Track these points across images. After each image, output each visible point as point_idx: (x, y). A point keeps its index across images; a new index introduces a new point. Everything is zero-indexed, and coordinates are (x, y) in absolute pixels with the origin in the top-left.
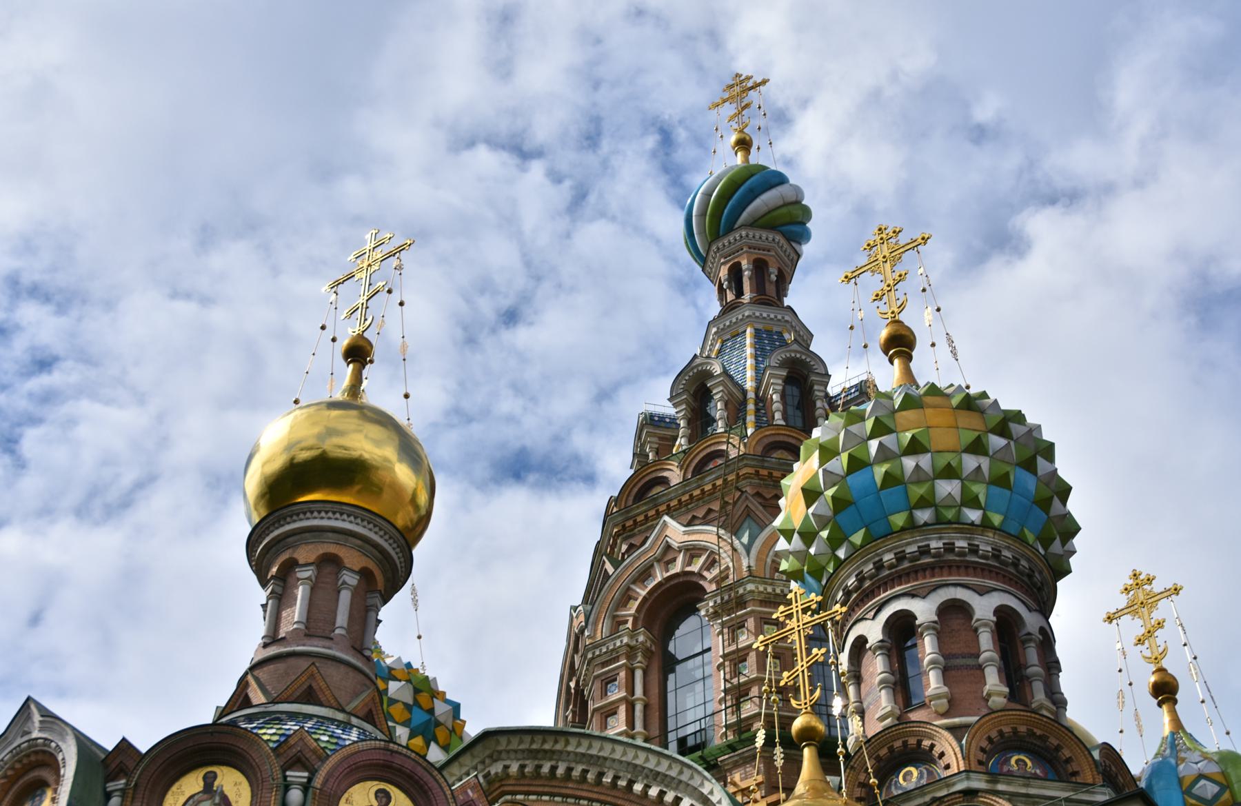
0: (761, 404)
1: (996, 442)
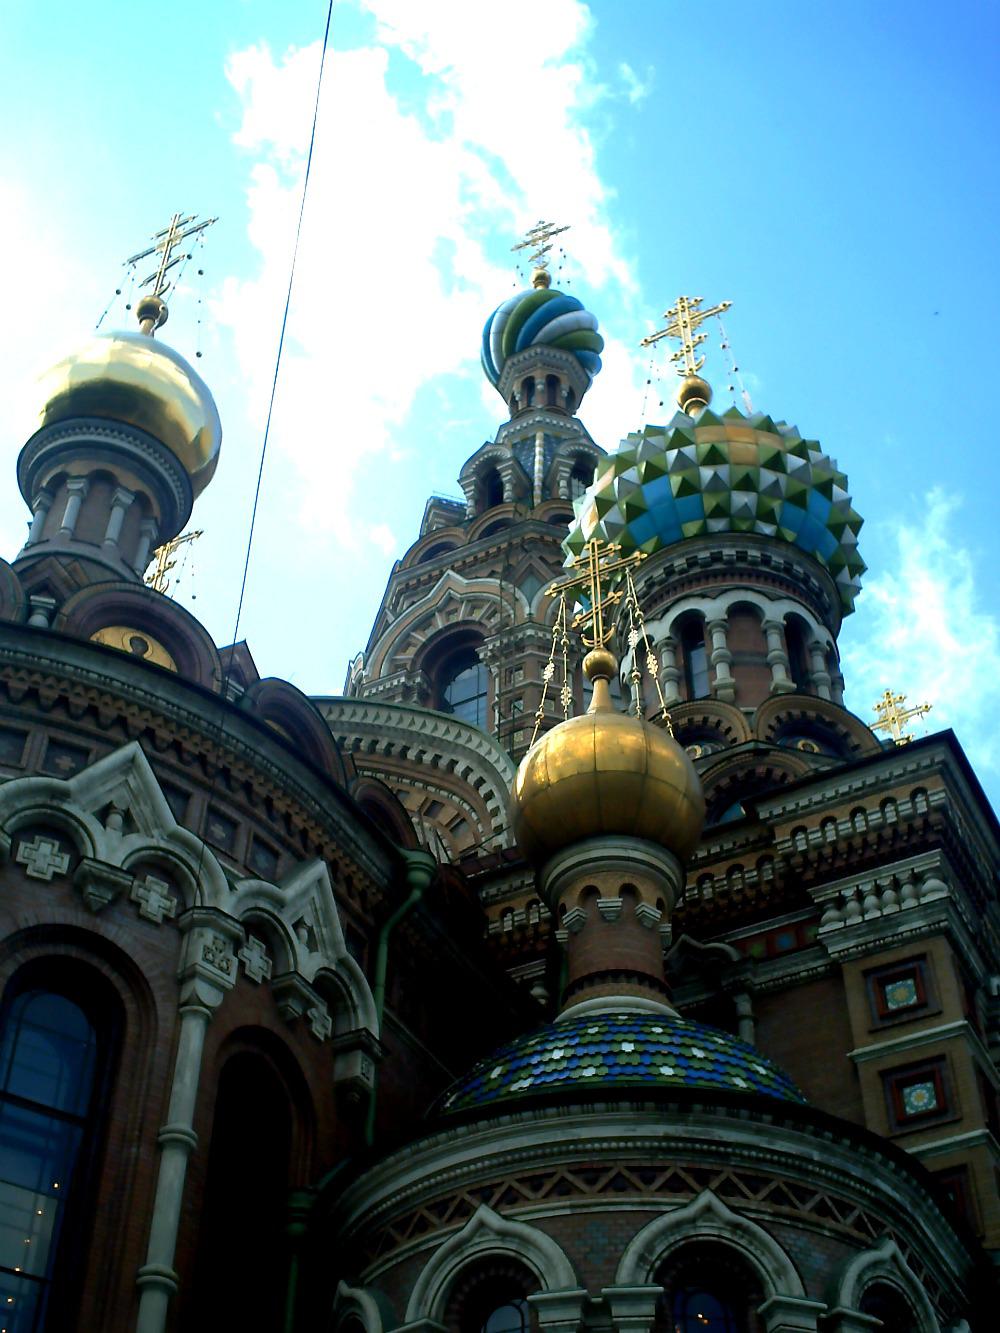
0: (547, 492)
1: (794, 462)
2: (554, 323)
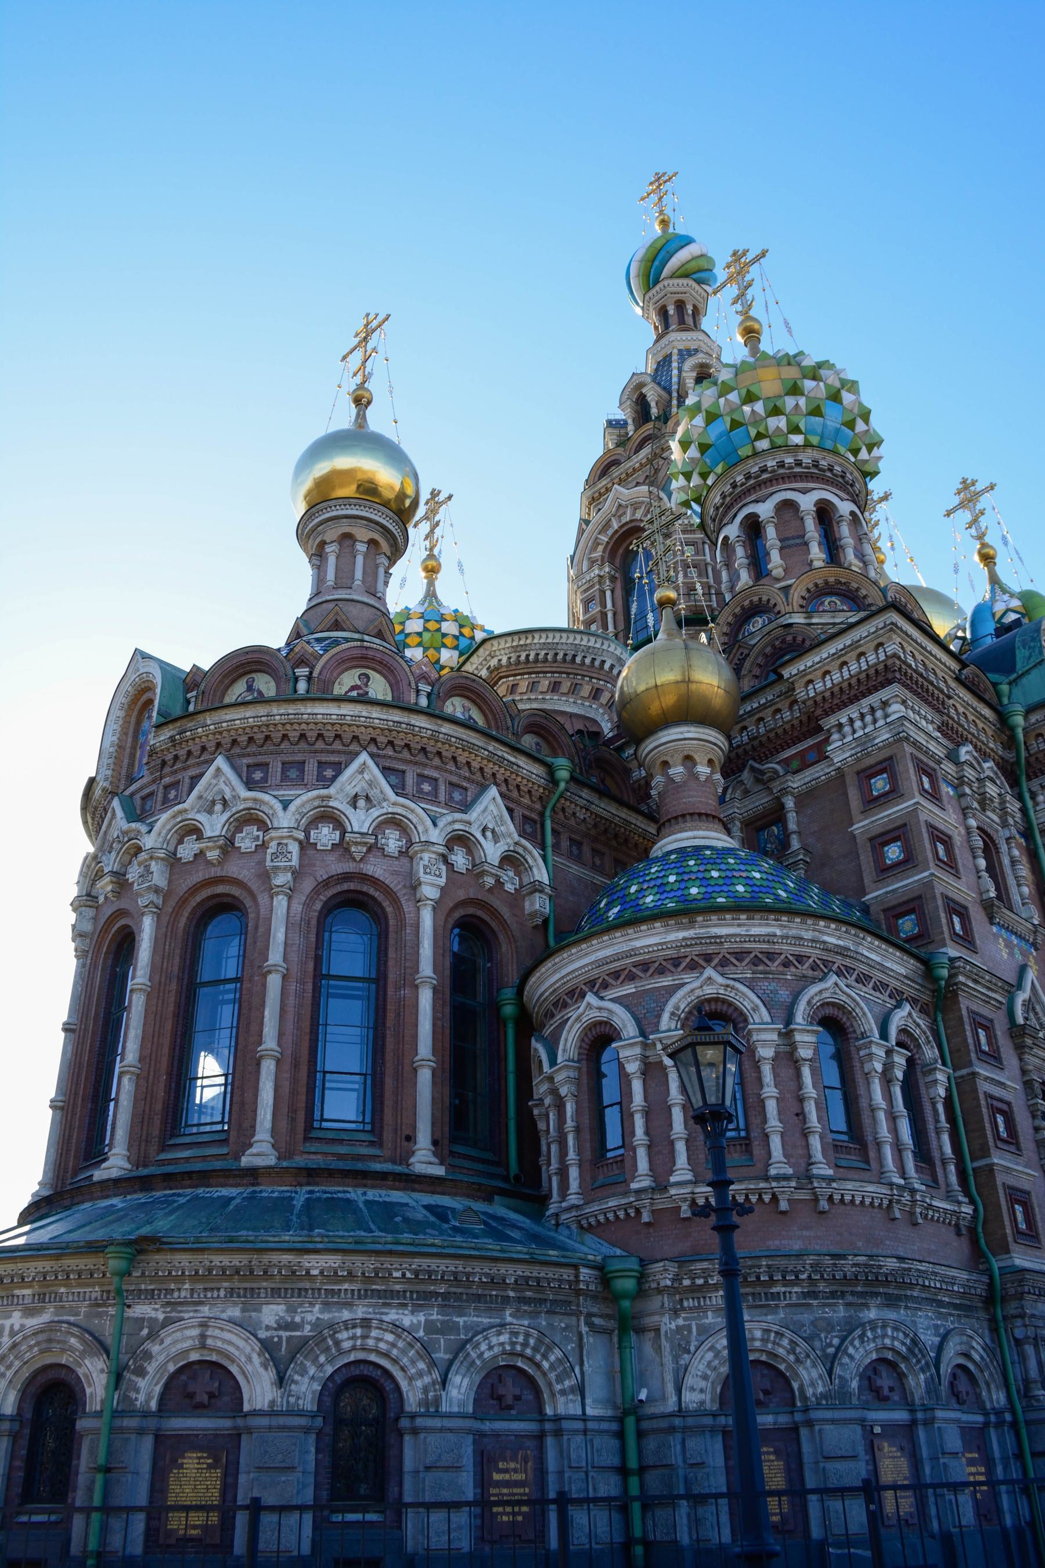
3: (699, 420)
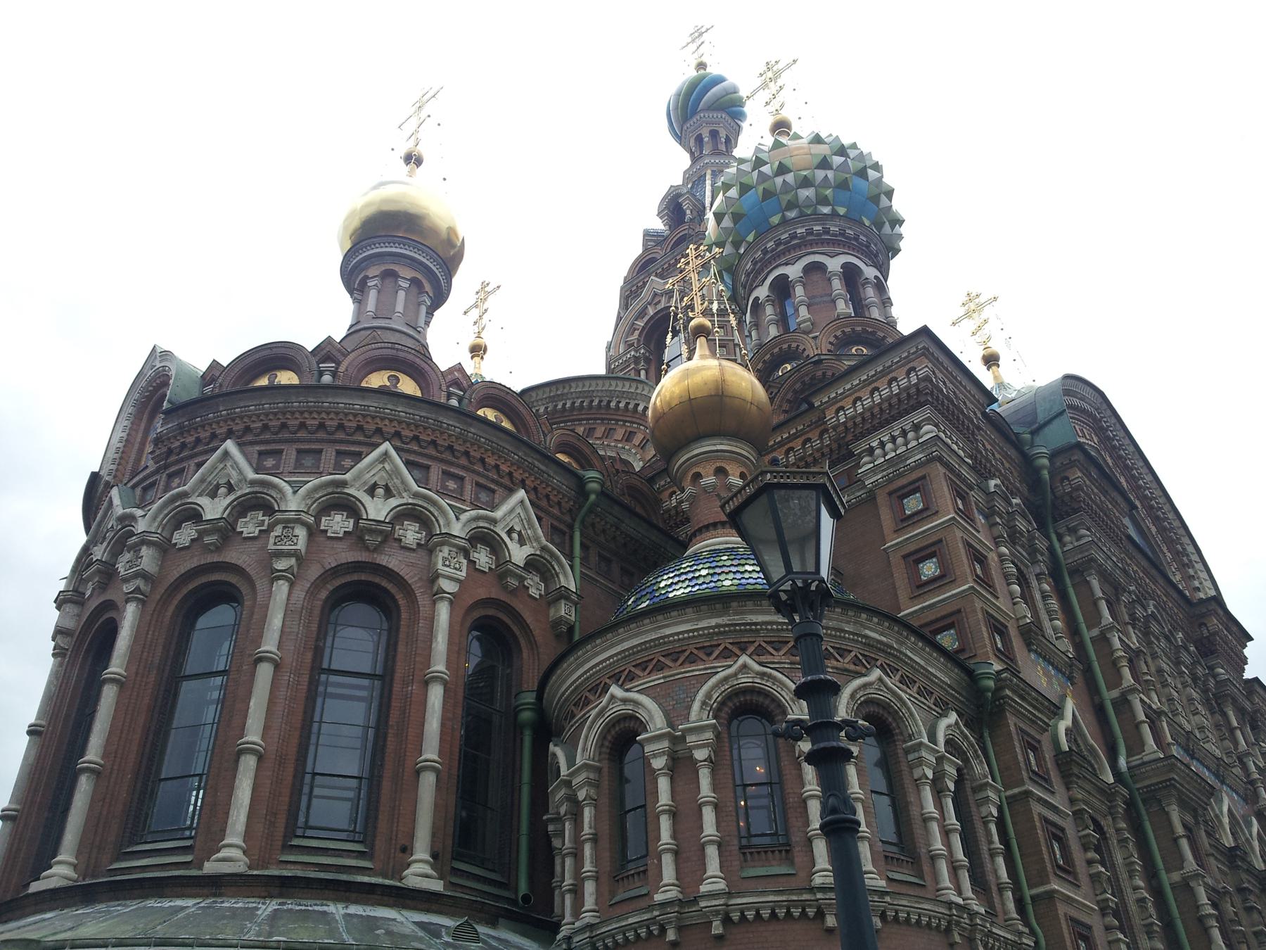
1: (838, 160)
2: (709, 93)
3: (733, 193)
